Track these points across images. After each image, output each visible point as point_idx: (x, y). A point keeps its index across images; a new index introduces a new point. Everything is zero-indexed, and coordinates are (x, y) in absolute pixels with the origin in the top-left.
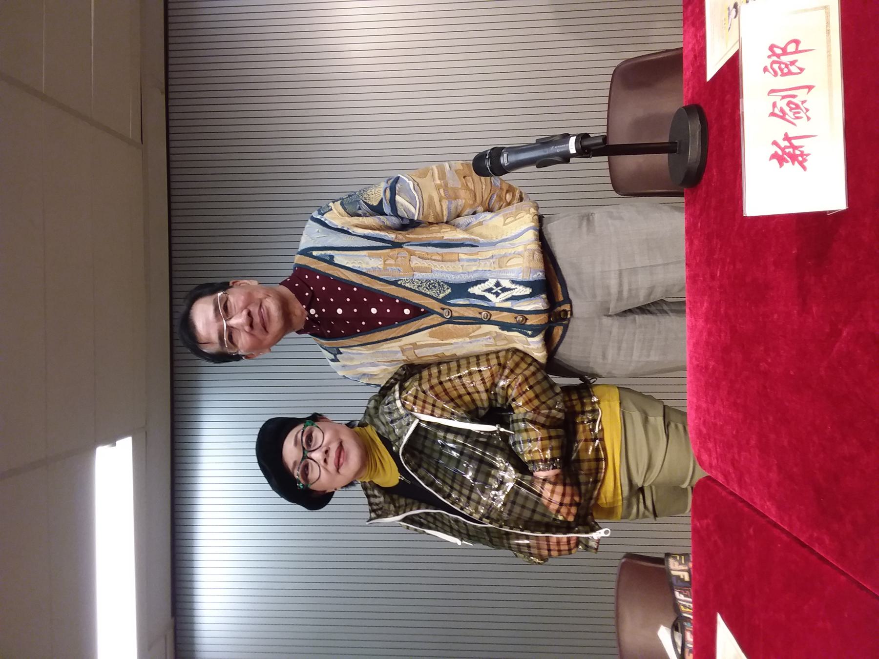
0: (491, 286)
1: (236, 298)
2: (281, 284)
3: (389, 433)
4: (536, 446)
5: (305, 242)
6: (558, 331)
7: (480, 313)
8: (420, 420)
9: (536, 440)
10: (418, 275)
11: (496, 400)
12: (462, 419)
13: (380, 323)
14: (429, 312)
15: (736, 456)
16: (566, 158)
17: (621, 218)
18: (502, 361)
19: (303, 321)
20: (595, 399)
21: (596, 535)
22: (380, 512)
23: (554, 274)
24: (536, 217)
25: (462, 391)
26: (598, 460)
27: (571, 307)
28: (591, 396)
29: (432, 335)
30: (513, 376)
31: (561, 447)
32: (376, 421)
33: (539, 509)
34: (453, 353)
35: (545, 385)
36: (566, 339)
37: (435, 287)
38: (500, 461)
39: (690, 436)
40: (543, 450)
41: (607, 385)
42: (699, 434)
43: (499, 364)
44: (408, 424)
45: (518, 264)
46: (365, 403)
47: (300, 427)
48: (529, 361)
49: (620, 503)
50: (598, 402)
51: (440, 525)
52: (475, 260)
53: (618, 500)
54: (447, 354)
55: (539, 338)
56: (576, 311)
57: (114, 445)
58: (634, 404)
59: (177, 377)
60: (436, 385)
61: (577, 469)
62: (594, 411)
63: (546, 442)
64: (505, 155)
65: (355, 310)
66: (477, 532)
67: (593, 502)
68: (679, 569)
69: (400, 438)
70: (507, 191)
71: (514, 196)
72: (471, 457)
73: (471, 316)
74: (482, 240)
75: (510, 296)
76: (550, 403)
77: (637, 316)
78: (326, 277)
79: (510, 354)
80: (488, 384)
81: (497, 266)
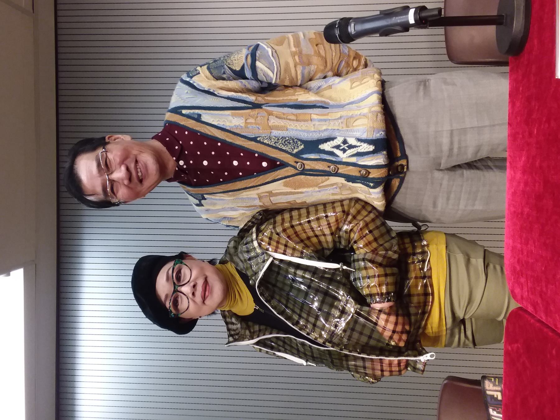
0: (339, 143)
1: (114, 153)
2: (152, 138)
3: (247, 269)
4: (373, 282)
5: (175, 102)
6: (396, 182)
7: (329, 167)
8: (274, 258)
9: (375, 275)
10: (275, 133)
11: (340, 242)
12: (310, 258)
13: (241, 174)
14: (284, 165)
15: (544, 289)
16: (406, 27)
17: (454, 84)
18: (346, 208)
19: (173, 171)
20: (425, 243)
21: (423, 358)
22: (237, 337)
23: (393, 132)
24: (380, 82)
25: (311, 234)
26: (426, 294)
27: (408, 162)
28: (421, 240)
29: (286, 185)
30: (355, 222)
31: (395, 284)
32: (236, 259)
33: (375, 336)
34: (304, 200)
35: (383, 229)
36: (402, 190)
37: (290, 143)
38: (341, 294)
39: (505, 272)
40: (380, 285)
41: (436, 232)
42: (513, 270)
43: (344, 211)
44: (264, 261)
45: (363, 125)
46: (226, 245)
47: (170, 265)
48: (369, 209)
49: (444, 333)
50: (428, 245)
51: (288, 348)
52: (325, 120)
53: (442, 331)
54: (299, 201)
55: (379, 190)
56: (411, 165)
57: (9, 275)
58: (459, 248)
59: (62, 218)
60: (288, 228)
61: (408, 303)
62: (424, 253)
63: (383, 279)
64: (352, 25)
65: (219, 163)
66: (320, 354)
67: (421, 331)
68: (493, 390)
69: (256, 273)
70: (355, 58)
71: (359, 62)
72: (317, 291)
73: (320, 169)
74: (331, 103)
75: (355, 152)
76: (387, 245)
77: (465, 171)
78: (193, 133)
79: (353, 204)
80: (333, 229)
81: (344, 125)
